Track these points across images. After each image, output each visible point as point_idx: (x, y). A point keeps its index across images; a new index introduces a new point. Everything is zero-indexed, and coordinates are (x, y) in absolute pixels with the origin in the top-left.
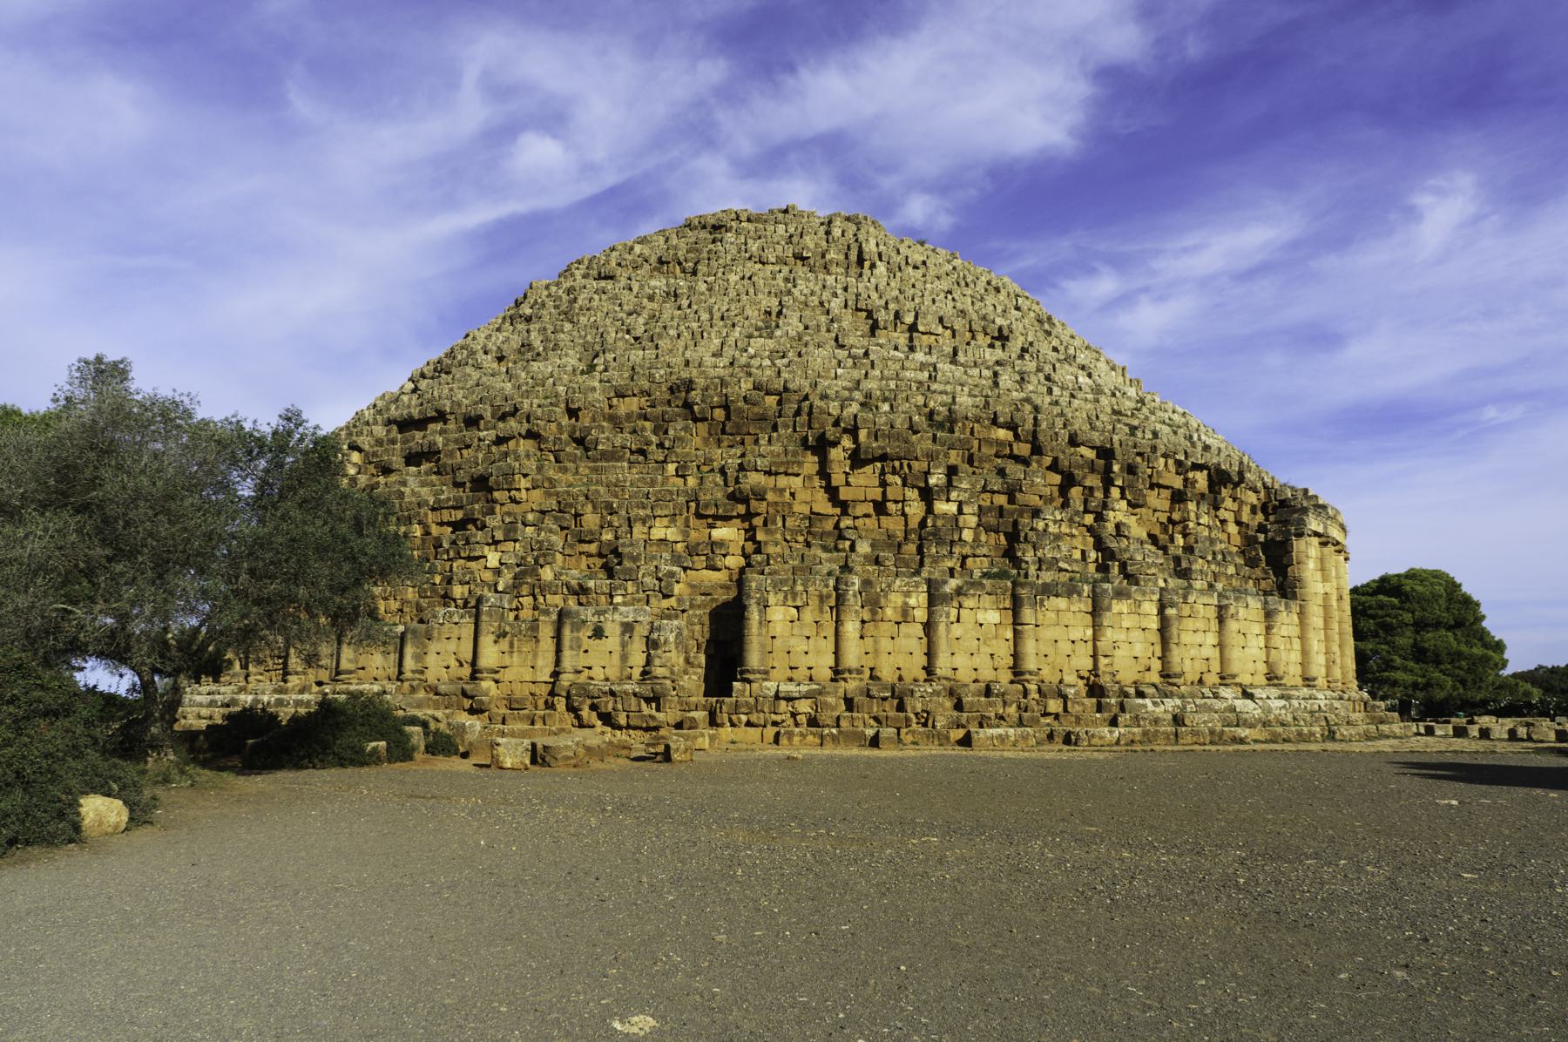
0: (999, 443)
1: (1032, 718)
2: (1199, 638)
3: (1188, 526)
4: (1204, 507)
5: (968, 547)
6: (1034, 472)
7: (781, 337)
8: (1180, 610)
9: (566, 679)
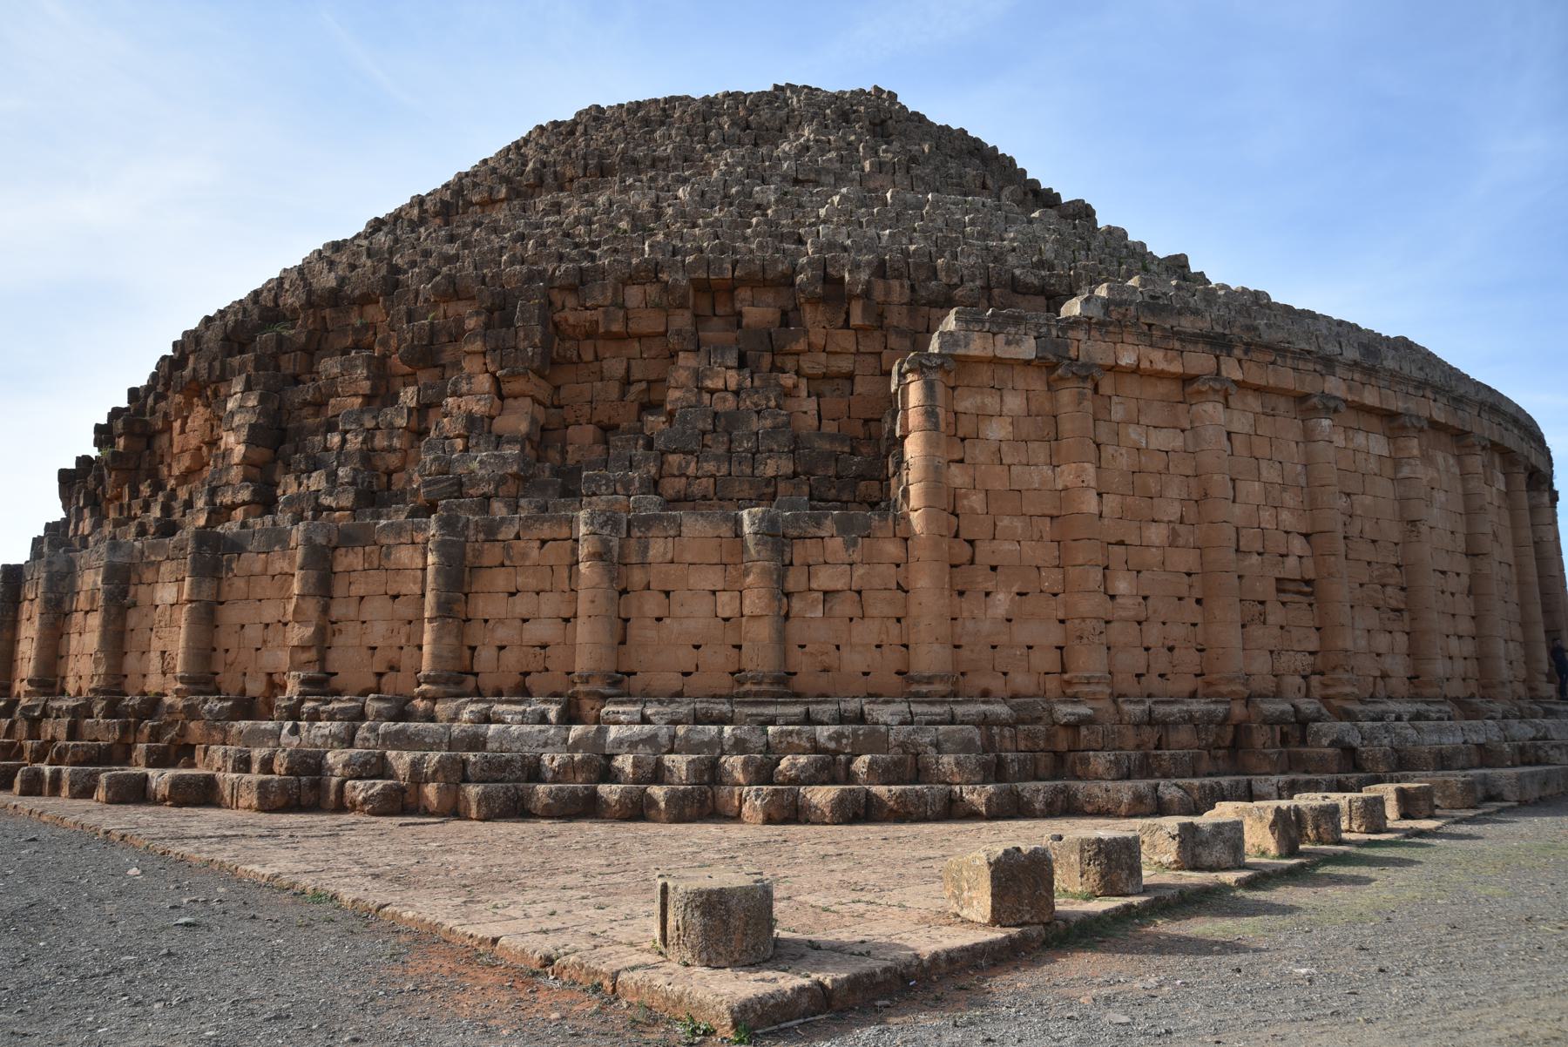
2: (522, 605)
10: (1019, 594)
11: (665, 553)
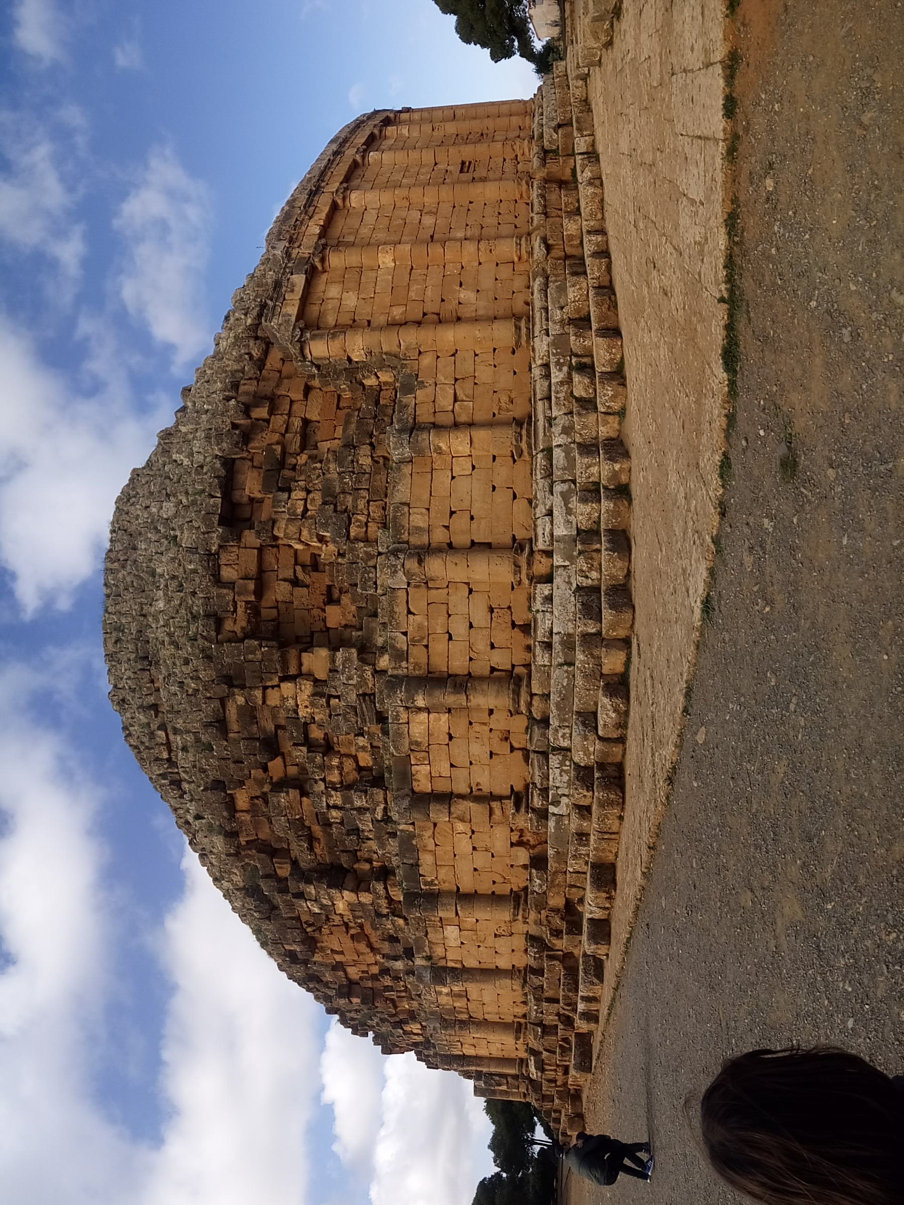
2: (459, 628)
10: (461, 285)
11: (422, 514)
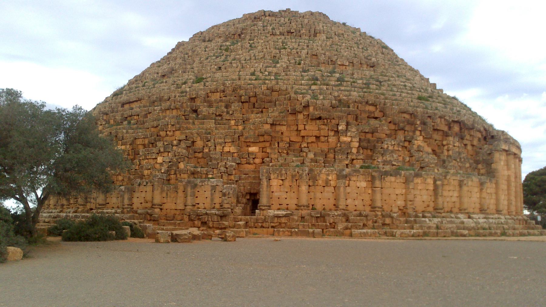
0: (370, 112)
1: (378, 226)
2: (451, 193)
3: (449, 147)
4: (457, 139)
5: (354, 156)
6: (383, 124)
7: (280, 67)
8: (443, 182)
9: (189, 208)
